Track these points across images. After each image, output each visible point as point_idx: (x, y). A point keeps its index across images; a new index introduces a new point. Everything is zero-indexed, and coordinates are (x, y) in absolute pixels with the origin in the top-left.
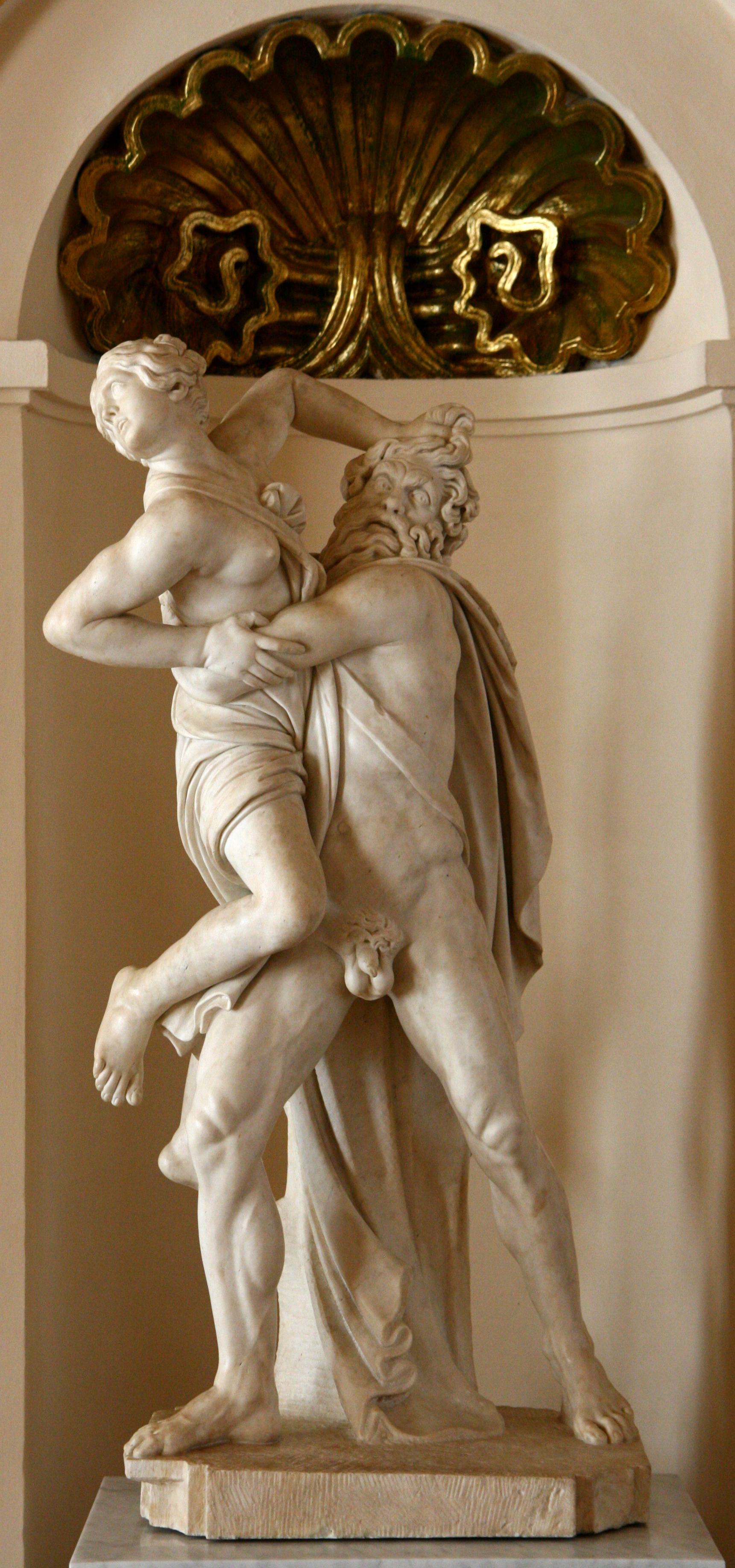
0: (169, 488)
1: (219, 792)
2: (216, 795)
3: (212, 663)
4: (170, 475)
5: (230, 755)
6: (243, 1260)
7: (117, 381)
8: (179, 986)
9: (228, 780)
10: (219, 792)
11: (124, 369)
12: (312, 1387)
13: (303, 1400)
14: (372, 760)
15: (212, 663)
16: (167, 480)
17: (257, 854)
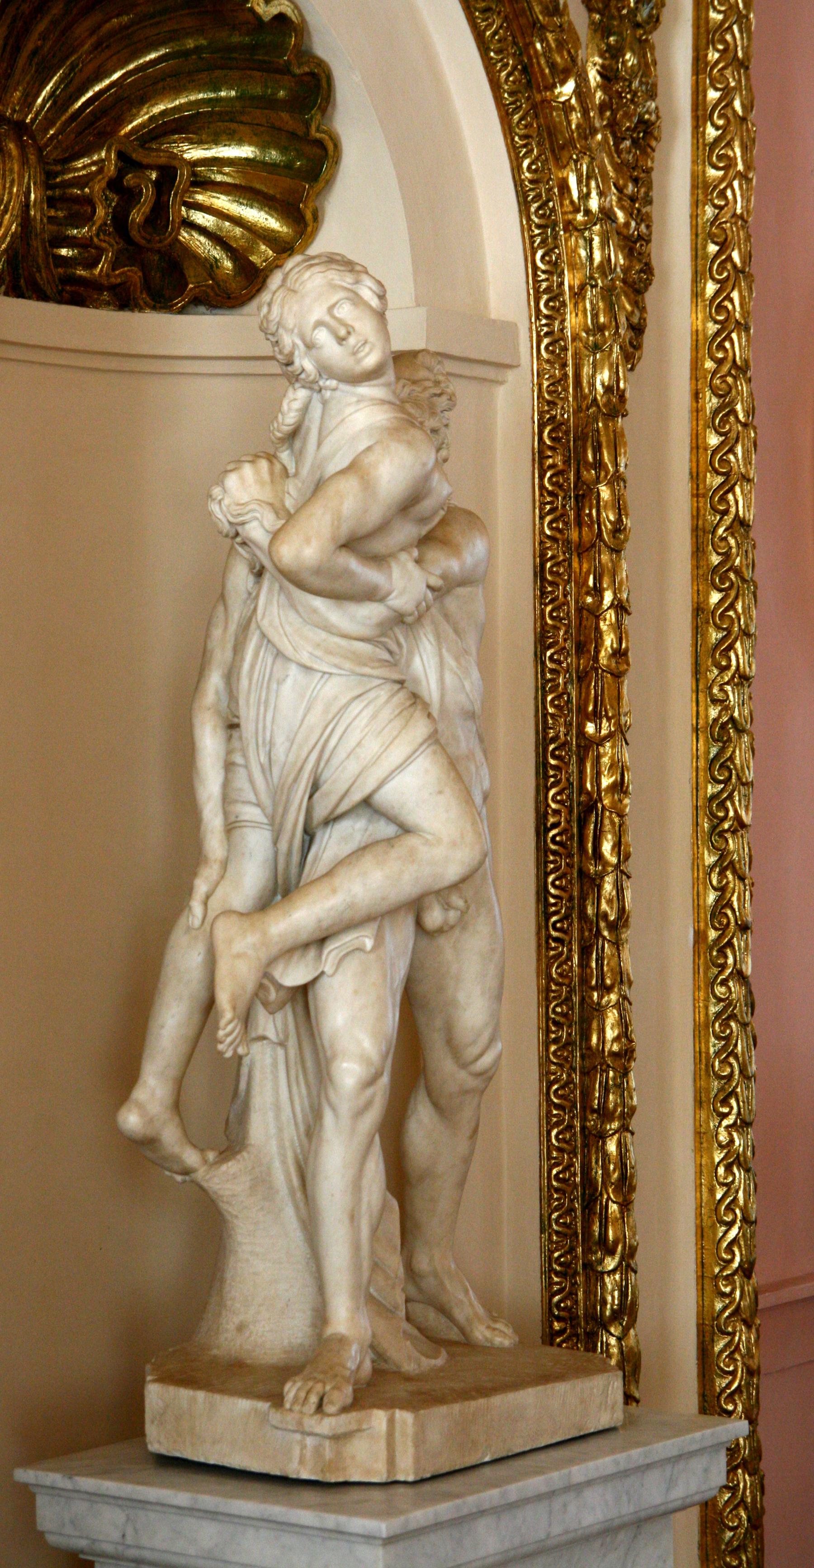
0: (392, 415)
1: (383, 729)
2: (380, 732)
3: (396, 598)
4: (383, 402)
5: (382, 693)
6: (369, 1202)
7: (347, 299)
8: (327, 929)
9: (393, 716)
10: (383, 729)
11: (349, 286)
12: (309, 1331)
13: (301, 1345)
14: (462, 698)
15: (396, 598)
16: (386, 407)
17: (440, 792)
